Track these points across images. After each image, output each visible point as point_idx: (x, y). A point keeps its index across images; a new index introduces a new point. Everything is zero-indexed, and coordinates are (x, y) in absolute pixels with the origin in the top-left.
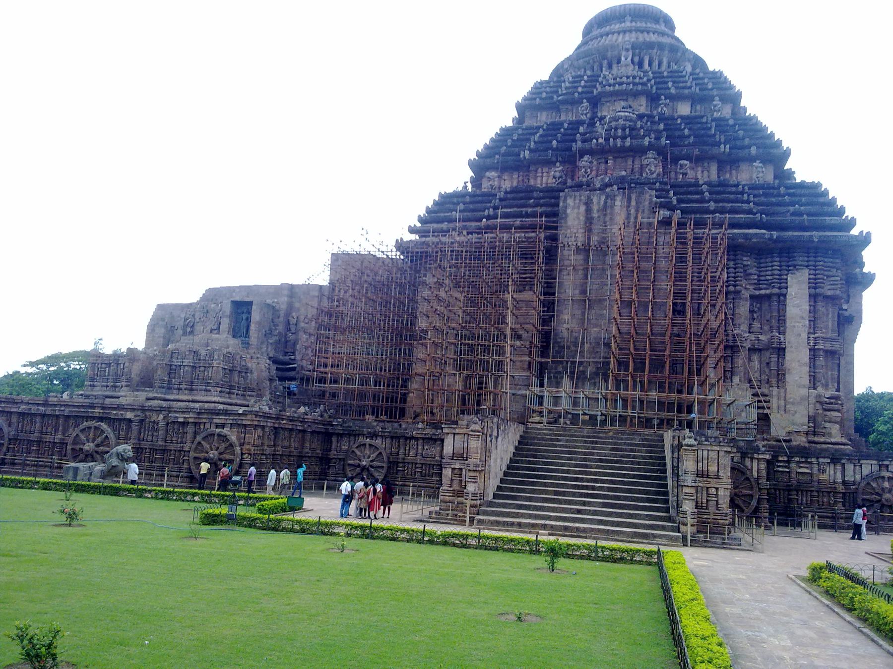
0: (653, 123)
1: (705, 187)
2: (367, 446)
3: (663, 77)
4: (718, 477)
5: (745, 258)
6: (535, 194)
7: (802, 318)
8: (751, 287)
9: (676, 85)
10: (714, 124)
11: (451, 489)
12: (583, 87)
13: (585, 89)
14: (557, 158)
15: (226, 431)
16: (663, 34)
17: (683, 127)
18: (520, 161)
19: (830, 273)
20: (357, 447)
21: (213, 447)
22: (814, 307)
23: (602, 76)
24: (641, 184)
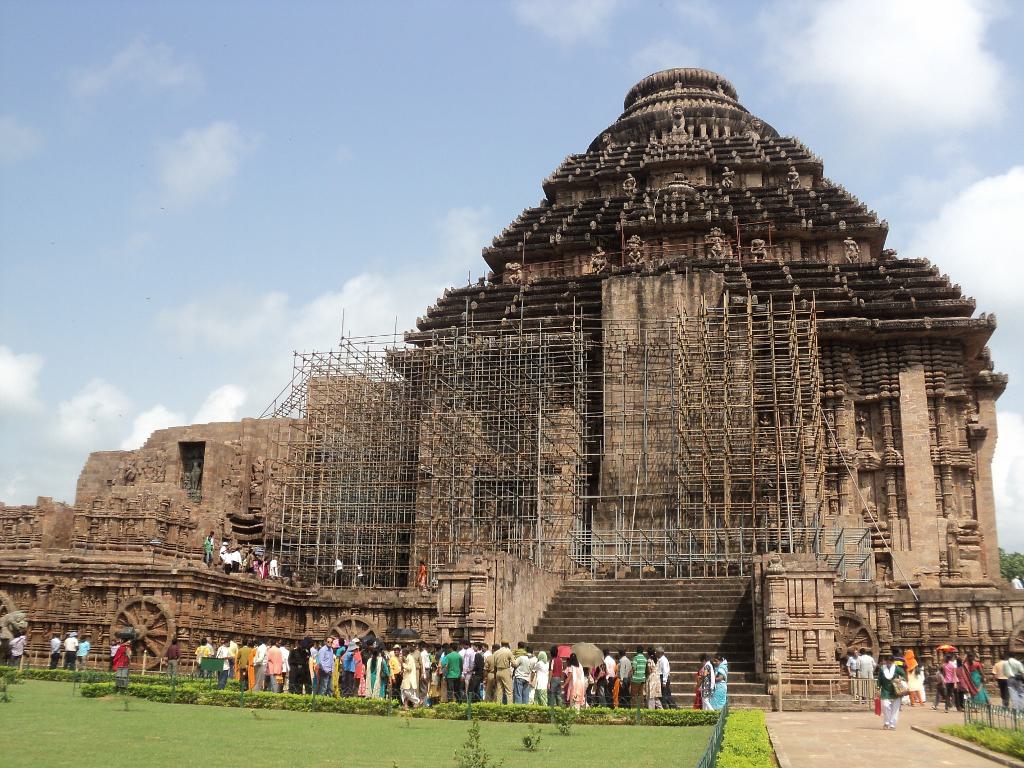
0: (716, 196)
2: (354, 623)
3: (725, 146)
4: (817, 615)
5: (843, 355)
6: (571, 285)
7: (921, 426)
13: (630, 162)
15: (157, 598)
16: (722, 101)
18: (551, 247)
19: (951, 369)
24: (705, 267)
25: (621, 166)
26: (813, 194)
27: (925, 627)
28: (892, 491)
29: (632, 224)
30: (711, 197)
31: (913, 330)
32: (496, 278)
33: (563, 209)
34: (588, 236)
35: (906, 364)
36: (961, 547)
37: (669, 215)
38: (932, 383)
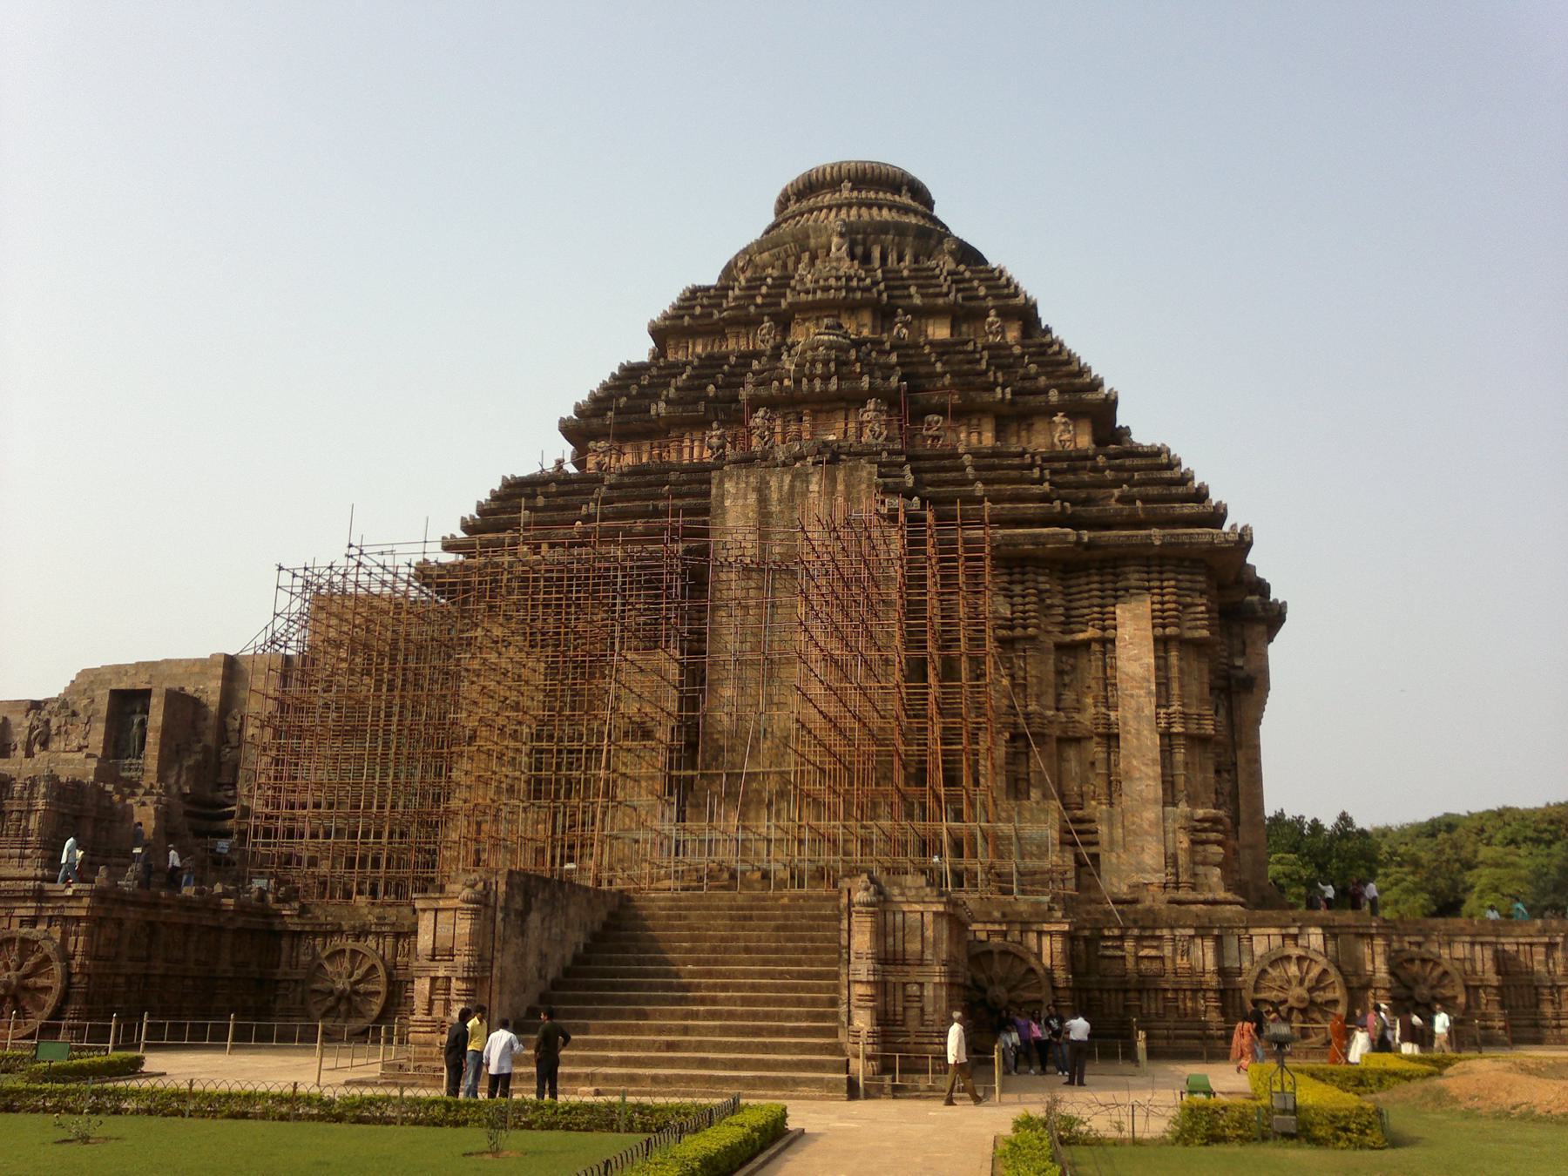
1: (967, 459)
3: (902, 278)
4: (921, 962)
5: (1041, 579)
6: (673, 476)
8: (1057, 629)
9: (924, 291)
10: (985, 353)
11: (429, 1018)
12: (764, 296)
13: (768, 300)
14: (716, 415)
16: (906, 210)
19: (1189, 600)
21: (12, 965)
22: (1166, 659)
23: (797, 277)
25: (757, 306)
26: (1017, 350)
29: (762, 391)
30: (874, 354)
31: (1136, 545)
34: (702, 406)
37: (811, 380)
38: (1159, 619)
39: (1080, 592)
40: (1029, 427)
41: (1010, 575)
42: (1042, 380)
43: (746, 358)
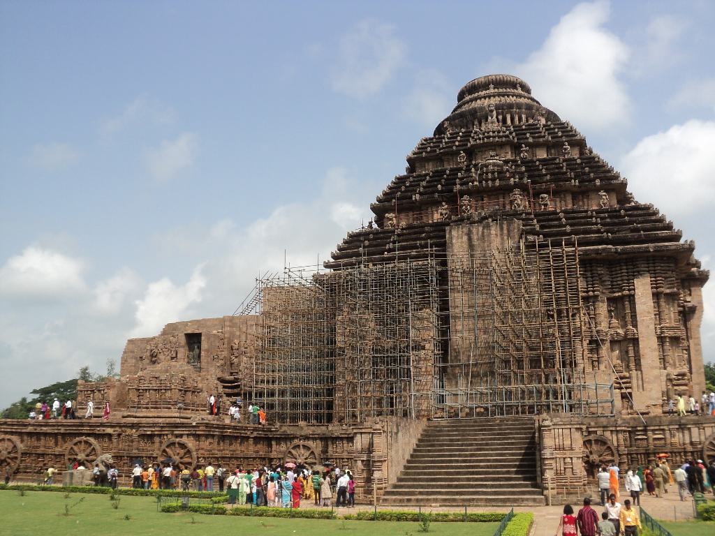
0: (517, 166)
1: (562, 215)
2: (301, 447)
3: (523, 130)
4: (572, 449)
5: (599, 269)
6: (426, 229)
9: (533, 135)
10: (565, 164)
13: (461, 143)
15: (184, 440)
16: (520, 96)
17: (541, 168)
18: (413, 202)
20: (292, 448)
24: (510, 215)
26: (579, 161)
27: (651, 441)
28: (631, 353)
29: (464, 187)
30: (513, 167)
31: (642, 252)
32: (380, 220)
33: (419, 176)
35: (638, 274)
36: (676, 388)
37: (487, 181)
38: (655, 285)
39: (617, 274)
40: (588, 197)
41: (585, 267)
42: (592, 175)
43: (454, 171)
